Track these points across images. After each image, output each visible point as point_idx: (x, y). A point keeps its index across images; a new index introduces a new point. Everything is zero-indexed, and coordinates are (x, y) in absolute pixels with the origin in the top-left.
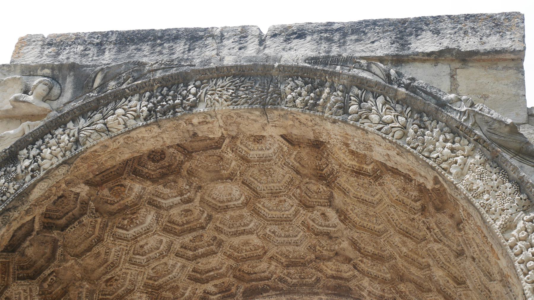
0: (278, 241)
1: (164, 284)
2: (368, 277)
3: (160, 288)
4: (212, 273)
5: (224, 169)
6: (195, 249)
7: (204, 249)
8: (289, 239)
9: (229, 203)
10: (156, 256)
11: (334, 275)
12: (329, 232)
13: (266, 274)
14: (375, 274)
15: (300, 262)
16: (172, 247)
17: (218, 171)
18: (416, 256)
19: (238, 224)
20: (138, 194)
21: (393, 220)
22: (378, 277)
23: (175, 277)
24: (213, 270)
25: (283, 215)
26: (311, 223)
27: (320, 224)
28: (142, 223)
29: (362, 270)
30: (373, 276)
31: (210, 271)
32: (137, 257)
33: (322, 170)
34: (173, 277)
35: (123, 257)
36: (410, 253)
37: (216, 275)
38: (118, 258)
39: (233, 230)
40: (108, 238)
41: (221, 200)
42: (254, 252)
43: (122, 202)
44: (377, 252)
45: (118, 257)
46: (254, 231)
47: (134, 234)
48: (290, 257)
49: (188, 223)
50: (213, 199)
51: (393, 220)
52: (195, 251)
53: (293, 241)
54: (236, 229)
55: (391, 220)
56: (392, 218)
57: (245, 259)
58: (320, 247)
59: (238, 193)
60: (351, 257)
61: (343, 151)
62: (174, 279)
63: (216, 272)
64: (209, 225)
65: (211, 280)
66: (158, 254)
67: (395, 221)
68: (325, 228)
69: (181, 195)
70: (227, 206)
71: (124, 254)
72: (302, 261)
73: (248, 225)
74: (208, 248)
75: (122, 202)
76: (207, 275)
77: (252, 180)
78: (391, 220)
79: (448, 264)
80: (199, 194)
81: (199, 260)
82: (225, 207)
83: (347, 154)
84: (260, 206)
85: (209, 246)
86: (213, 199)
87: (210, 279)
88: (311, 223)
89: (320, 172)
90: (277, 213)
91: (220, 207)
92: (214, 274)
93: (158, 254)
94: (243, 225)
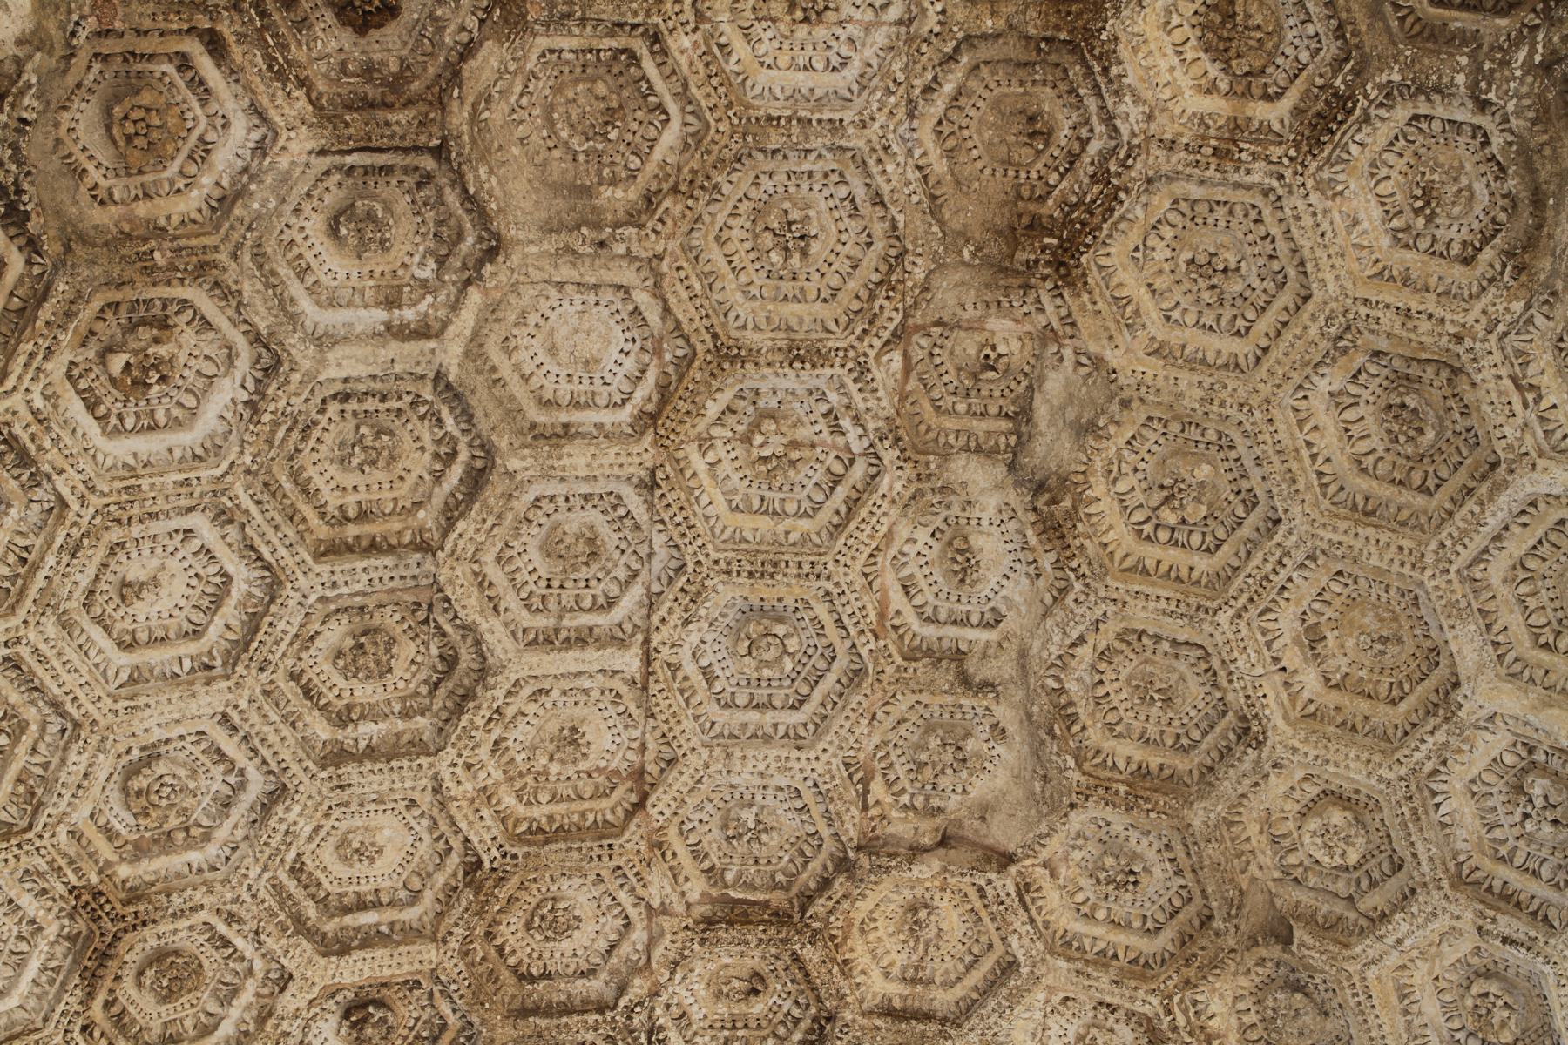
0: (717, 728)
1: (159, 886)
2: (1069, 959)
3: (138, 899)
4: (368, 918)
5: (614, 182)
6: (343, 719)
7: (382, 726)
8: (769, 717)
9: (577, 416)
10: (177, 670)
11: (897, 1004)
12: (964, 647)
13: (596, 987)
14: (1101, 945)
15: (765, 905)
16: (268, 619)
17: (587, 192)
18: (1364, 705)
19: (568, 598)
20: (225, 183)
21: (1314, 457)
22: (1115, 956)
23: (213, 868)
24: (378, 905)
25: (787, 533)
26: (897, 599)
27: (929, 610)
28: (176, 424)
29: (1047, 925)
30: (1089, 956)
31: (362, 905)
32: (96, 633)
33: (1042, 199)
34: (205, 867)
35: (51, 560)
36: (1334, 698)
37: (384, 929)
38: (22, 570)
39: (542, 622)
40: (26, 383)
41: (548, 395)
42: (586, 805)
43: (142, 209)
44: (1154, 761)
45: (24, 561)
46: (633, 635)
47: (132, 462)
48: (729, 876)
49: (364, 515)
50: (517, 367)
51: (1314, 457)
52: (344, 725)
53: (781, 730)
54: (552, 622)
55: (1305, 453)
56: (1309, 444)
57: (541, 837)
58: (889, 785)
59: (630, 364)
60: (1011, 848)
61: (1178, 36)
62: (209, 875)
63: (390, 915)
64: (461, 525)
65: (362, 947)
66: (187, 664)
67: (1320, 460)
68: (952, 631)
69: (391, 303)
70: (566, 426)
71: (59, 541)
72: (776, 898)
73: (611, 602)
74: (400, 725)
75: (142, 209)
76: (349, 920)
77: (721, 262)
78: (1305, 453)
79: (1544, 656)
80: (475, 296)
81: (350, 769)
82: (559, 430)
83: (1189, 56)
84: (698, 463)
85: (406, 714)
86: (517, 367)
87: (356, 943)
88: (897, 599)
89: (1032, 207)
90: (764, 523)
91: (533, 426)
92: (378, 924)
93: (187, 664)
94: (587, 603)
